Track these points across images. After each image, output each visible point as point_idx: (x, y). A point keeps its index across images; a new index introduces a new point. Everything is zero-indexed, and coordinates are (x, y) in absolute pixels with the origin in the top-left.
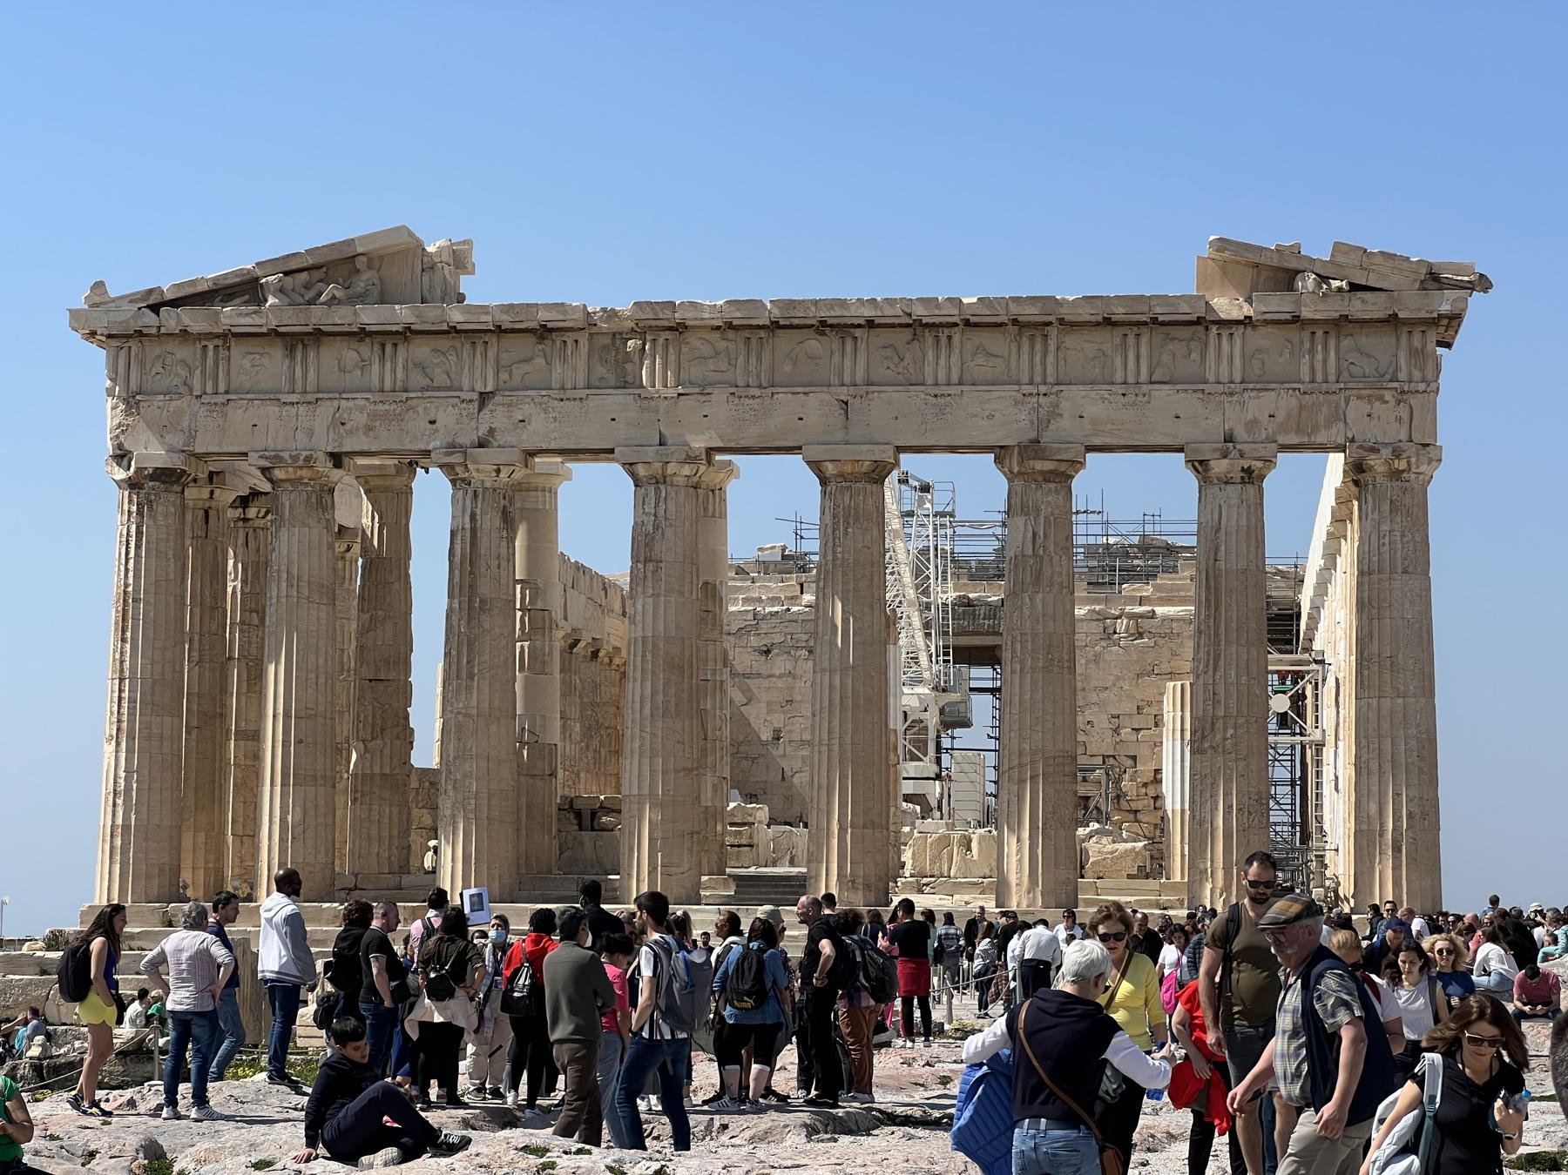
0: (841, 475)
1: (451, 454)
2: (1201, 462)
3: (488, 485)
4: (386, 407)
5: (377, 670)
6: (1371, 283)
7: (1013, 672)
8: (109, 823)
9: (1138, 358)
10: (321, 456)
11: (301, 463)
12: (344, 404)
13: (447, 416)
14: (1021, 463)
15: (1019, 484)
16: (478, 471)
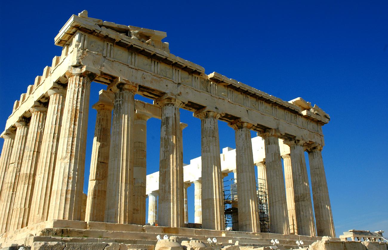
0: (247, 127)
1: (172, 95)
2: (298, 141)
3: (178, 107)
4: (155, 78)
5: (104, 159)
6: (319, 114)
7: (277, 178)
8: (65, 189)
9: (289, 117)
10: (138, 85)
11: (134, 85)
12: (145, 72)
13: (171, 85)
14: (275, 133)
15: (273, 138)
16: (178, 102)
